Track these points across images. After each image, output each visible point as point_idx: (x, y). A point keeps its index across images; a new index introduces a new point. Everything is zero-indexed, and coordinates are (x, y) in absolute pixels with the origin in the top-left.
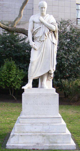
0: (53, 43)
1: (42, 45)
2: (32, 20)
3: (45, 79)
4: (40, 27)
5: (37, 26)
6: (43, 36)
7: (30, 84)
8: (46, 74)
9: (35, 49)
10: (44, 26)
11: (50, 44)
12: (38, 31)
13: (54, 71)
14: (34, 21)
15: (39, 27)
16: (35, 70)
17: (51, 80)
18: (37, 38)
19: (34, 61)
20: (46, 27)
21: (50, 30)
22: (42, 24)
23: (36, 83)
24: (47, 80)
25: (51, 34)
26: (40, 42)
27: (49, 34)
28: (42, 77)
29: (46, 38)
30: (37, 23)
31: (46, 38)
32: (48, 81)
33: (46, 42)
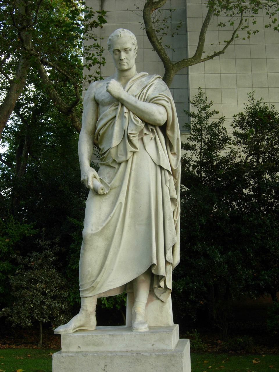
0: (162, 168)
3: (143, 294)
4: (114, 115)
8: (143, 278)
11: (149, 173)
18: (105, 155)
20: (131, 113)
21: (147, 124)
23: (113, 312)
24: (149, 301)
25: (151, 135)
26: (116, 166)
27: (145, 138)
28: (130, 289)
29: (134, 150)
31: (134, 150)
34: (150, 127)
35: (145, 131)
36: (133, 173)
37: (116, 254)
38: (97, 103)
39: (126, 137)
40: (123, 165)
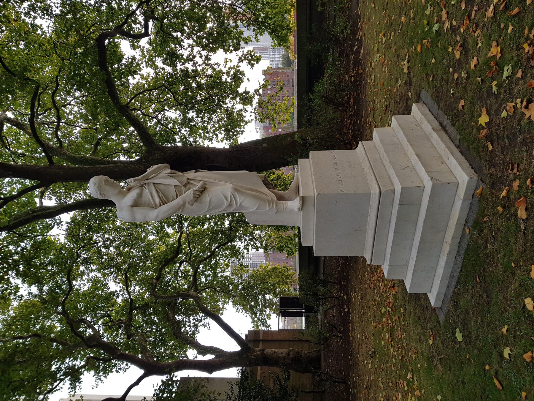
4: (152, 184)
12: (162, 187)
30: (140, 195)
38: (136, 204)
40: (190, 181)
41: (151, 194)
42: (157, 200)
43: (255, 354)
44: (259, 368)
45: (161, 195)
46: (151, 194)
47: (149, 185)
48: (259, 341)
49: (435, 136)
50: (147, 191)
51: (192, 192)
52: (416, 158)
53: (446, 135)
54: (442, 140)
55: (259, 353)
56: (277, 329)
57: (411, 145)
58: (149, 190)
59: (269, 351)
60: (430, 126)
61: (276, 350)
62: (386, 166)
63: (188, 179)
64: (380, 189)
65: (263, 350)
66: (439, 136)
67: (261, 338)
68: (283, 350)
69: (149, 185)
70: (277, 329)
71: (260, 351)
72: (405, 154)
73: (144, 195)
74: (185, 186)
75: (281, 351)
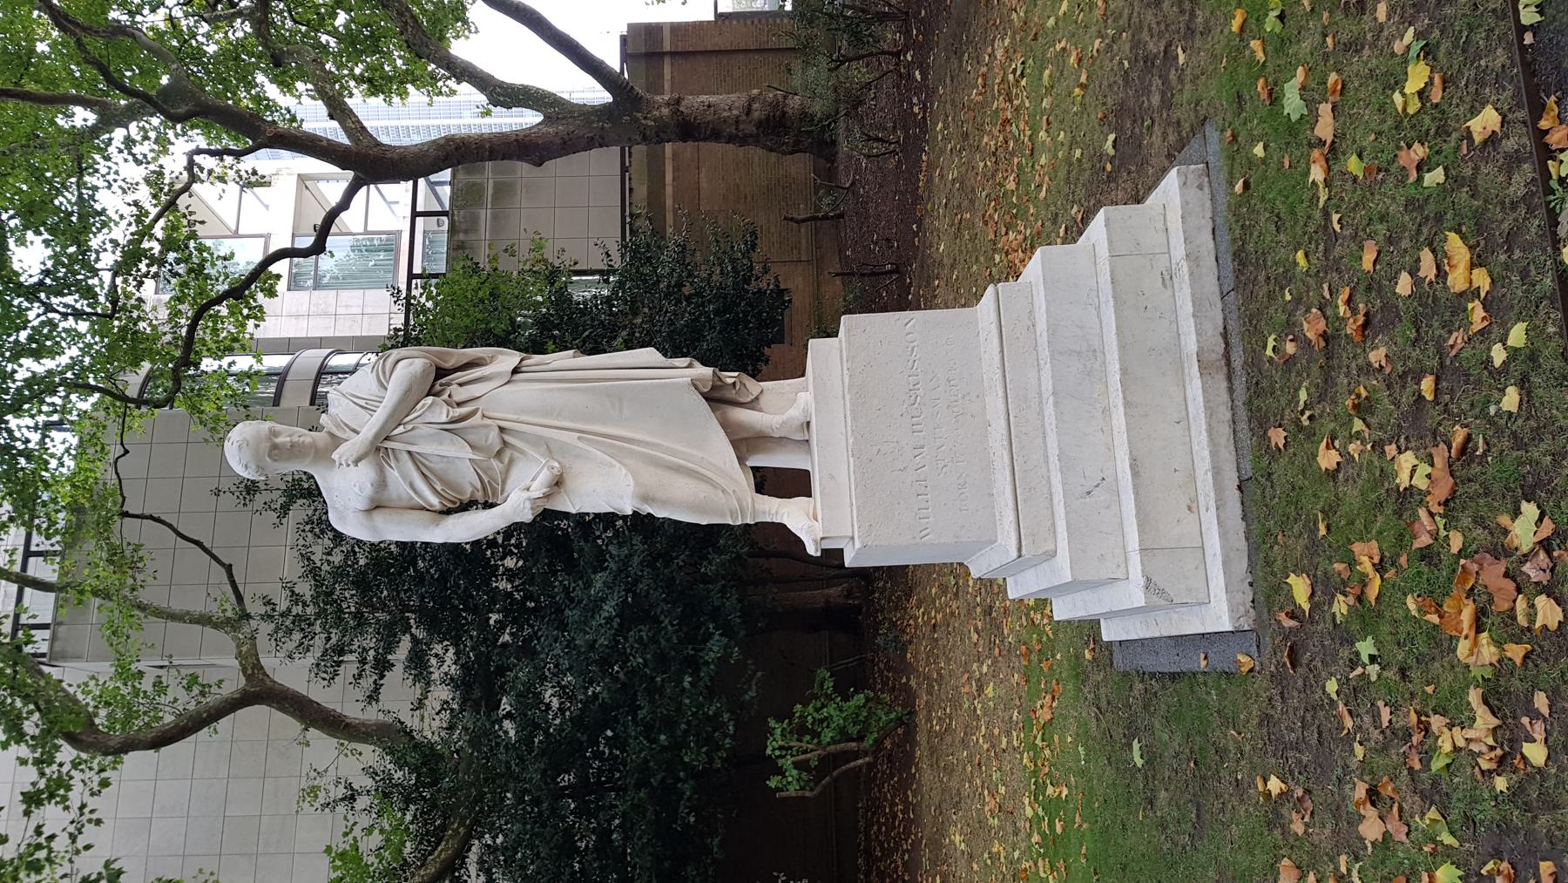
0: (516, 371)
1: (537, 441)
2: (361, 515)
4: (406, 456)
5: (402, 480)
6: (471, 438)
7: (791, 514)
9: (558, 483)
10: (401, 429)
11: (523, 391)
12: (438, 466)
13: (696, 364)
14: (362, 504)
15: (410, 465)
16: (703, 485)
17: (754, 387)
19: (637, 484)
22: (388, 444)
27: (457, 398)
28: (745, 442)
29: (479, 414)
30: (381, 483)
32: (763, 401)
33: (514, 417)
34: (438, 387)
35: (445, 396)
36: (523, 418)
37: (673, 453)
38: (376, 506)
39: (453, 427)
40: (507, 438)
41: (412, 486)
42: (435, 501)
43: (656, 113)
44: (668, 147)
45: (439, 488)
46: (412, 486)
47: (397, 459)
48: (662, 55)
49: (1195, 386)
50: (396, 473)
51: (528, 505)
52: (1129, 471)
53: (1225, 397)
54: (1210, 430)
55: (665, 111)
56: (712, 18)
57: (1127, 404)
58: (400, 472)
59: (695, 102)
60: (1194, 337)
61: (712, 99)
62: (1049, 441)
63: (502, 429)
64: (1020, 549)
65: (678, 102)
66: (1207, 401)
67: (667, 47)
68: (733, 97)
69: (397, 459)
70: (712, 18)
71: (668, 104)
72: (1106, 411)
73: (390, 482)
74: (499, 454)
75: (726, 101)
